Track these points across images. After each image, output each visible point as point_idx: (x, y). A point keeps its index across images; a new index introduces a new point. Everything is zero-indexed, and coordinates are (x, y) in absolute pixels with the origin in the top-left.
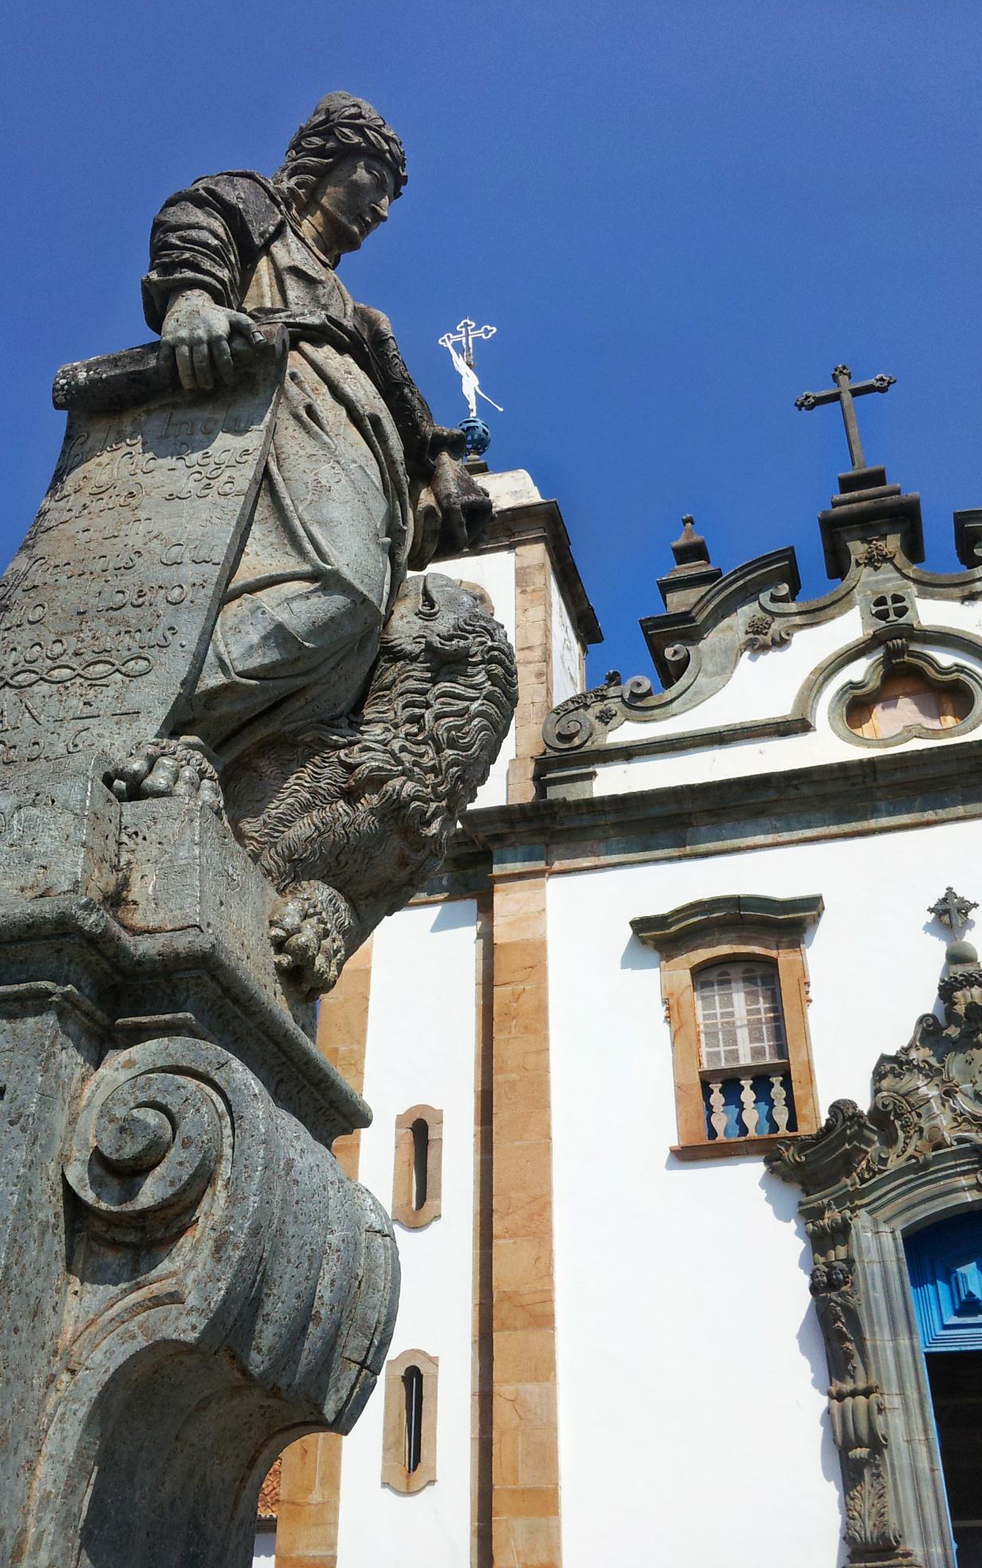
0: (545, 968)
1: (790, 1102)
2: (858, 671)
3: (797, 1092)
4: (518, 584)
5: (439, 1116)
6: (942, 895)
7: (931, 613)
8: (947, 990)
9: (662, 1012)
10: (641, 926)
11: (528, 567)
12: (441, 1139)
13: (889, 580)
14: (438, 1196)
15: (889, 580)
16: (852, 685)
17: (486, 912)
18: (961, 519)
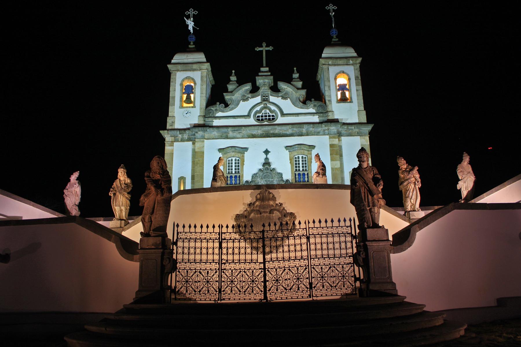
1: (239, 180)
3: (241, 178)
4: (201, 80)
6: (265, 149)
11: (203, 76)
13: (266, 92)
15: (266, 92)
17: (194, 145)
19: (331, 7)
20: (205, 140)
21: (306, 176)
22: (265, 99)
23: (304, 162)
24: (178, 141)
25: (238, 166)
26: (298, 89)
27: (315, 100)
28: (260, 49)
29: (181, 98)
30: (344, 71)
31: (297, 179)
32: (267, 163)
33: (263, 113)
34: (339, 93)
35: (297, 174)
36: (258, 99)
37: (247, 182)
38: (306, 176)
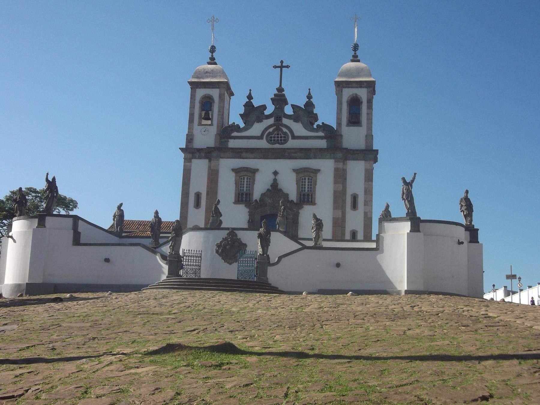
0: (218, 174)
2: (271, 130)
4: (219, 98)
5: (201, 194)
6: (275, 170)
7: (285, 121)
8: (271, 186)
9: (234, 182)
10: (233, 170)
12: (201, 197)
14: (200, 205)
16: (270, 132)
18: (292, 105)
20: (221, 160)
21: (310, 197)
23: (310, 184)
25: (249, 184)
29: (200, 115)
30: (358, 94)
31: (302, 199)
32: (275, 185)
33: (276, 134)
35: (302, 195)
36: (271, 121)
37: (256, 200)
38: (310, 197)
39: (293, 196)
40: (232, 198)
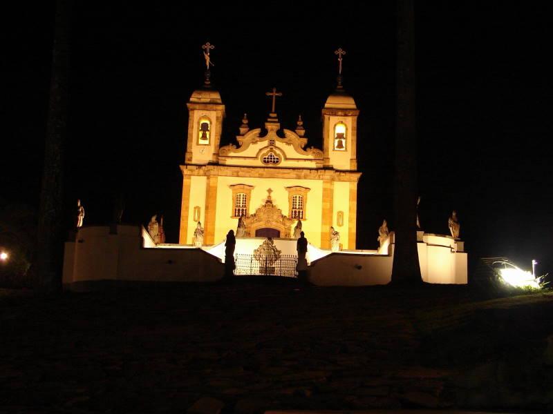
2: (265, 151)
19: (340, 52)
20: (219, 177)
22: (272, 143)
24: (194, 175)
26: (301, 137)
27: (314, 148)
28: (271, 94)
32: (269, 202)
34: (337, 141)
36: (266, 143)
39: (286, 213)
40: (230, 212)
